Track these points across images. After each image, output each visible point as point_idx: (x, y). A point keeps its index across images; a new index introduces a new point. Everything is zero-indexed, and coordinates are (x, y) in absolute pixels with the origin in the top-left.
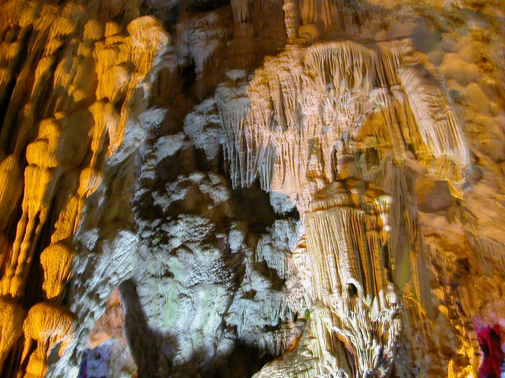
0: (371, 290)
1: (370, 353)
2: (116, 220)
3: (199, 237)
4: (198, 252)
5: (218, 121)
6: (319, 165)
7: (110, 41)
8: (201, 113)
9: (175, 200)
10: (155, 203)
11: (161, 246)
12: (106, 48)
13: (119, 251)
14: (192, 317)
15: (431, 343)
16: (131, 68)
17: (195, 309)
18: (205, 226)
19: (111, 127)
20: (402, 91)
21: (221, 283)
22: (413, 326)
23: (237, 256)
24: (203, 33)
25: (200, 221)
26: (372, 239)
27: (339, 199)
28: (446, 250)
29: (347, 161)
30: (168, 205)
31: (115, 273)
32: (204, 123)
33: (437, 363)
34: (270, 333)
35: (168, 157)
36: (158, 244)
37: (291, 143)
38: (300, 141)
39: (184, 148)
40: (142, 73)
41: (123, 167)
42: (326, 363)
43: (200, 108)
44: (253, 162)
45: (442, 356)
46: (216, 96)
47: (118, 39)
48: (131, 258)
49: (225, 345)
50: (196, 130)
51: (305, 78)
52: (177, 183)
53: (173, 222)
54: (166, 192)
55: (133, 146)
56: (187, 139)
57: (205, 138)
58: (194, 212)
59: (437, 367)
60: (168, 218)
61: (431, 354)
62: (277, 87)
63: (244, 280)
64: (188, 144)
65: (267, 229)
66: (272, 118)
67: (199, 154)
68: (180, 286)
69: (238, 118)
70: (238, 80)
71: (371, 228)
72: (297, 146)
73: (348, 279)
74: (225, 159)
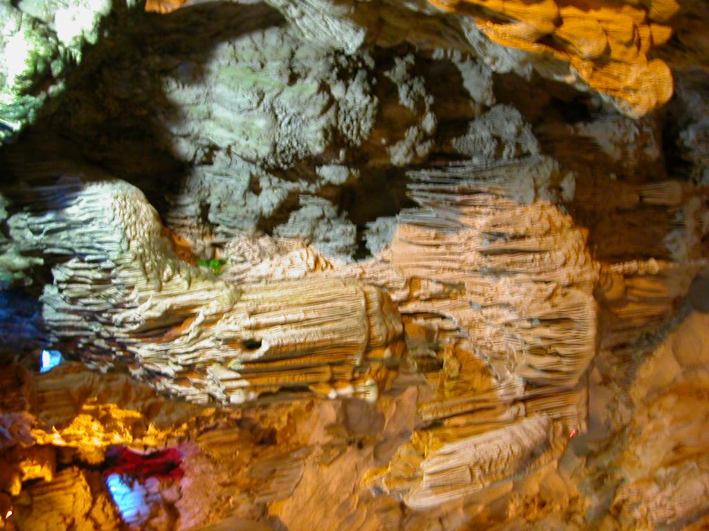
0: (250, 371)
1: (165, 361)
2: (381, 22)
3: (343, 125)
4: (323, 122)
7: (645, 32)
8: (519, 133)
9: (400, 90)
10: (397, 60)
12: (635, 27)
13: (335, 25)
16: (601, 61)
19: (516, 28)
20: (516, 418)
21: (274, 152)
23: (310, 173)
24: (632, 138)
25: (366, 126)
27: (379, 332)
28: (290, 416)
29: (429, 332)
30: (394, 80)
31: (303, 14)
32: (504, 137)
33: (138, 395)
34: (199, 211)
35: (461, 80)
36: (338, 64)
37: (462, 257)
39: (472, 104)
40: (591, 77)
41: (458, 36)
42: (154, 302)
43: (527, 132)
46: (542, 158)
47: (645, 44)
48: (322, 38)
49: (186, 149)
50: (498, 124)
51: (551, 287)
53: (368, 89)
54: (413, 77)
55: (486, 55)
56: (485, 109)
57: (484, 136)
58: (380, 120)
59: (133, 395)
60: (374, 81)
62: (543, 247)
64: (477, 109)
65: (345, 213)
70: (560, 190)
72: (456, 265)
73: (269, 339)
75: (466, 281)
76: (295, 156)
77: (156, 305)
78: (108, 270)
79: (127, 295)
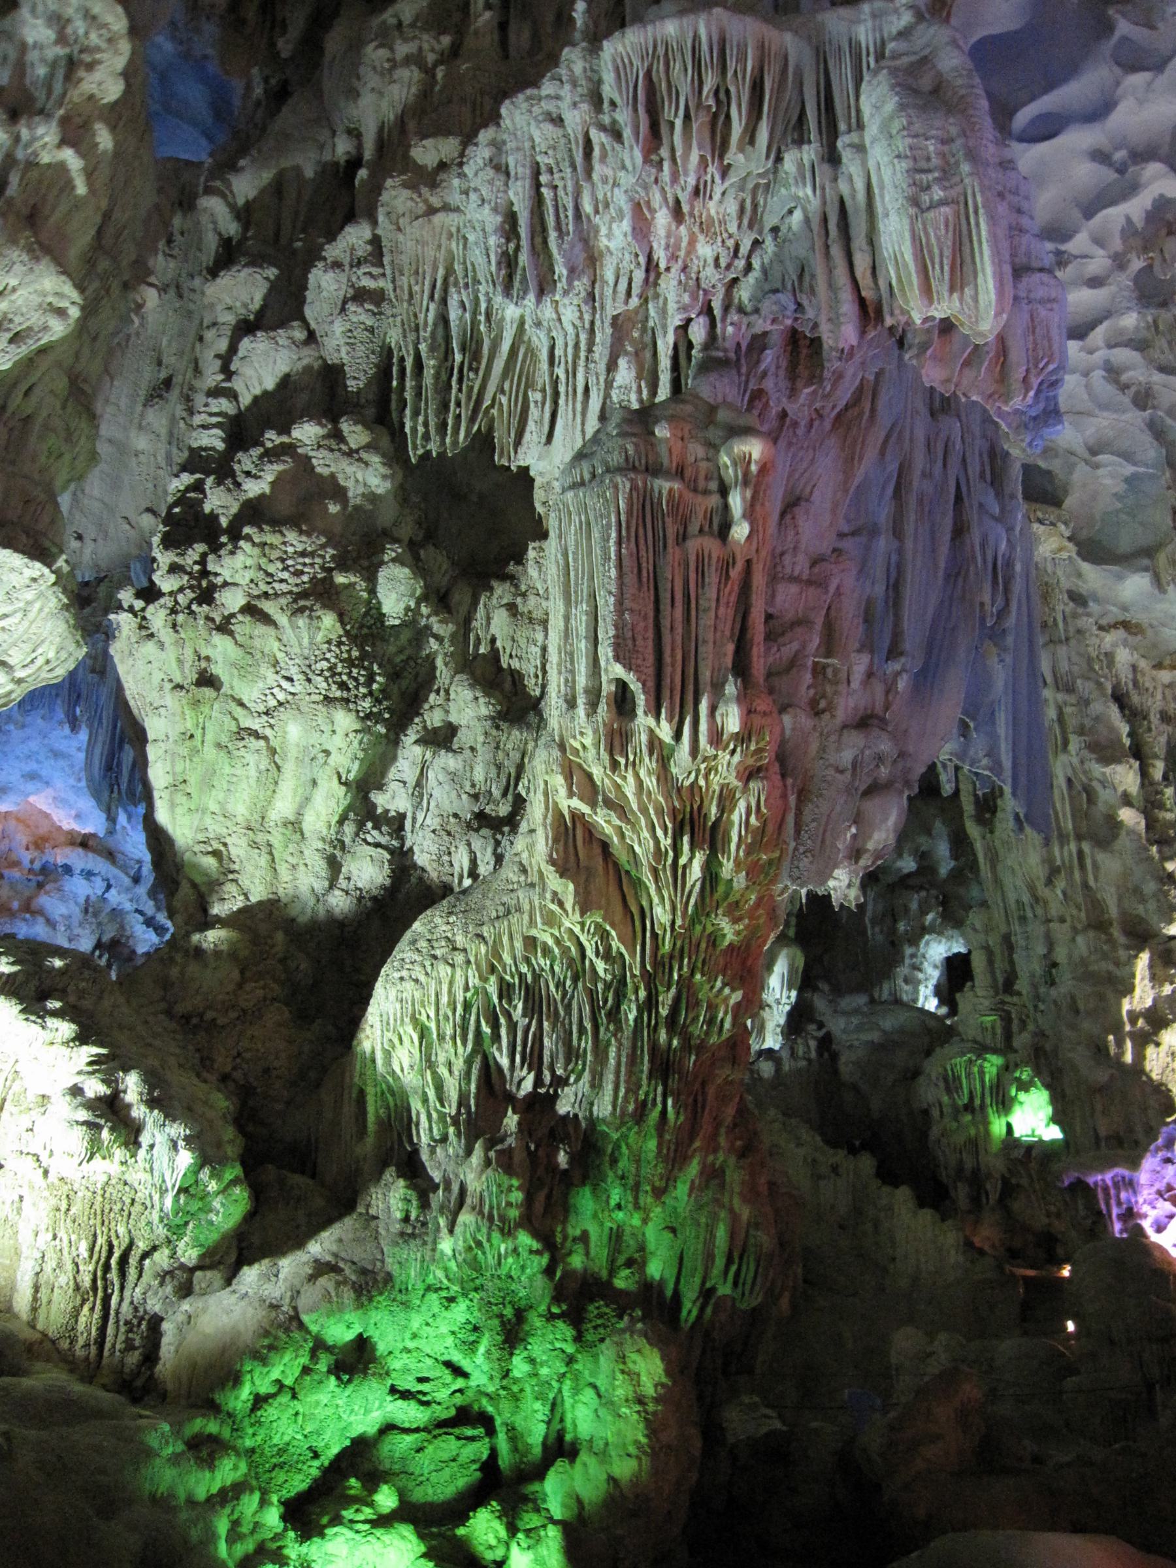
1: (678, 873)
3: (292, 583)
5: (381, 283)
6: (639, 387)
8: (337, 265)
9: (251, 495)
10: (207, 508)
11: (194, 607)
14: (272, 787)
15: (1095, 905)
17: (278, 768)
18: (312, 554)
21: (347, 701)
22: (1049, 860)
23: (405, 635)
25: (294, 540)
26: (700, 560)
28: (1159, 666)
29: (709, 365)
30: (234, 510)
32: (344, 290)
33: (1105, 956)
34: (485, 832)
35: (266, 393)
37: (570, 330)
38: (592, 323)
42: (548, 896)
43: (333, 251)
44: (471, 389)
45: (1122, 939)
51: (597, 136)
52: (262, 450)
54: (233, 474)
59: (1105, 966)
61: (1091, 934)
62: (525, 172)
63: (432, 697)
65: (512, 568)
66: (509, 262)
67: (332, 374)
68: (239, 709)
69: (428, 269)
71: (701, 531)
72: (583, 337)
74: (395, 383)
75: (610, 311)
76: (350, 663)
77: (555, 893)
78: (505, 990)
79: (547, 951)
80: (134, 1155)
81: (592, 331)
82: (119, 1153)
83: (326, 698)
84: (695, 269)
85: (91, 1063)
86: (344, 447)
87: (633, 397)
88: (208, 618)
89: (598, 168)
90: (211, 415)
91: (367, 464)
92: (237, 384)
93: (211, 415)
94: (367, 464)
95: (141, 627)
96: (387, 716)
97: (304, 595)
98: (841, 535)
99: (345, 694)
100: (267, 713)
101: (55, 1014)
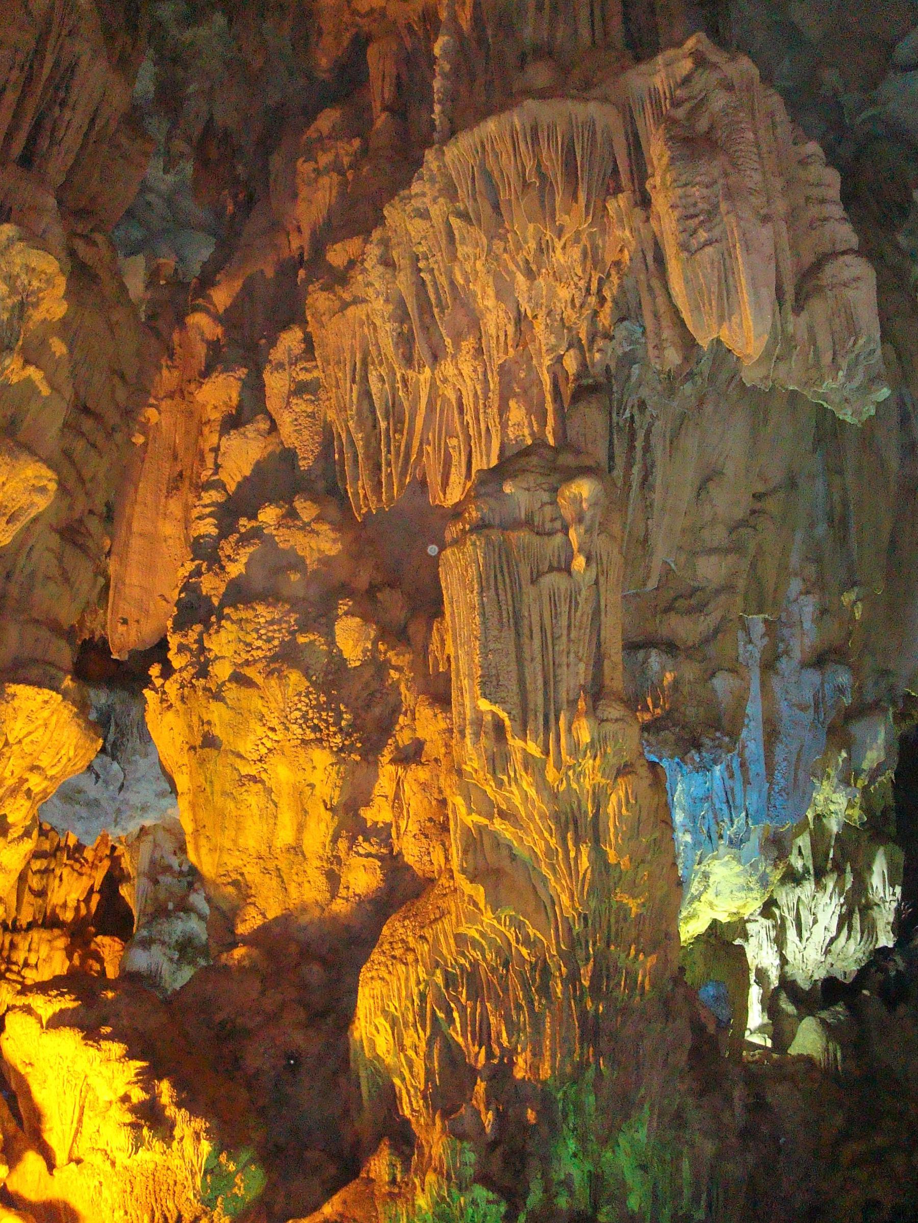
5: (316, 374)
8: (280, 366)
9: (233, 576)
11: (194, 681)
14: (272, 821)
18: (279, 622)
21: (320, 740)
30: (222, 590)
35: (246, 479)
43: (278, 354)
51: (455, 222)
54: (218, 560)
63: (401, 719)
67: (289, 456)
68: (238, 760)
69: (348, 356)
74: (337, 456)
76: (319, 708)
77: (470, 897)
78: (450, 980)
79: (475, 944)
80: (169, 1146)
81: (486, 381)
82: (158, 1145)
83: (303, 741)
84: (559, 311)
85: (137, 1075)
86: (299, 523)
87: (526, 432)
88: (206, 689)
89: (462, 250)
90: (205, 506)
91: (318, 534)
92: (223, 476)
93: (205, 506)
94: (318, 534)
95: (162, 701)
96: (359, 745)
97: (274, 659)
98: (757, 497)
99: (318, 735)
100: (260, 761)
101: (107, 1037)
